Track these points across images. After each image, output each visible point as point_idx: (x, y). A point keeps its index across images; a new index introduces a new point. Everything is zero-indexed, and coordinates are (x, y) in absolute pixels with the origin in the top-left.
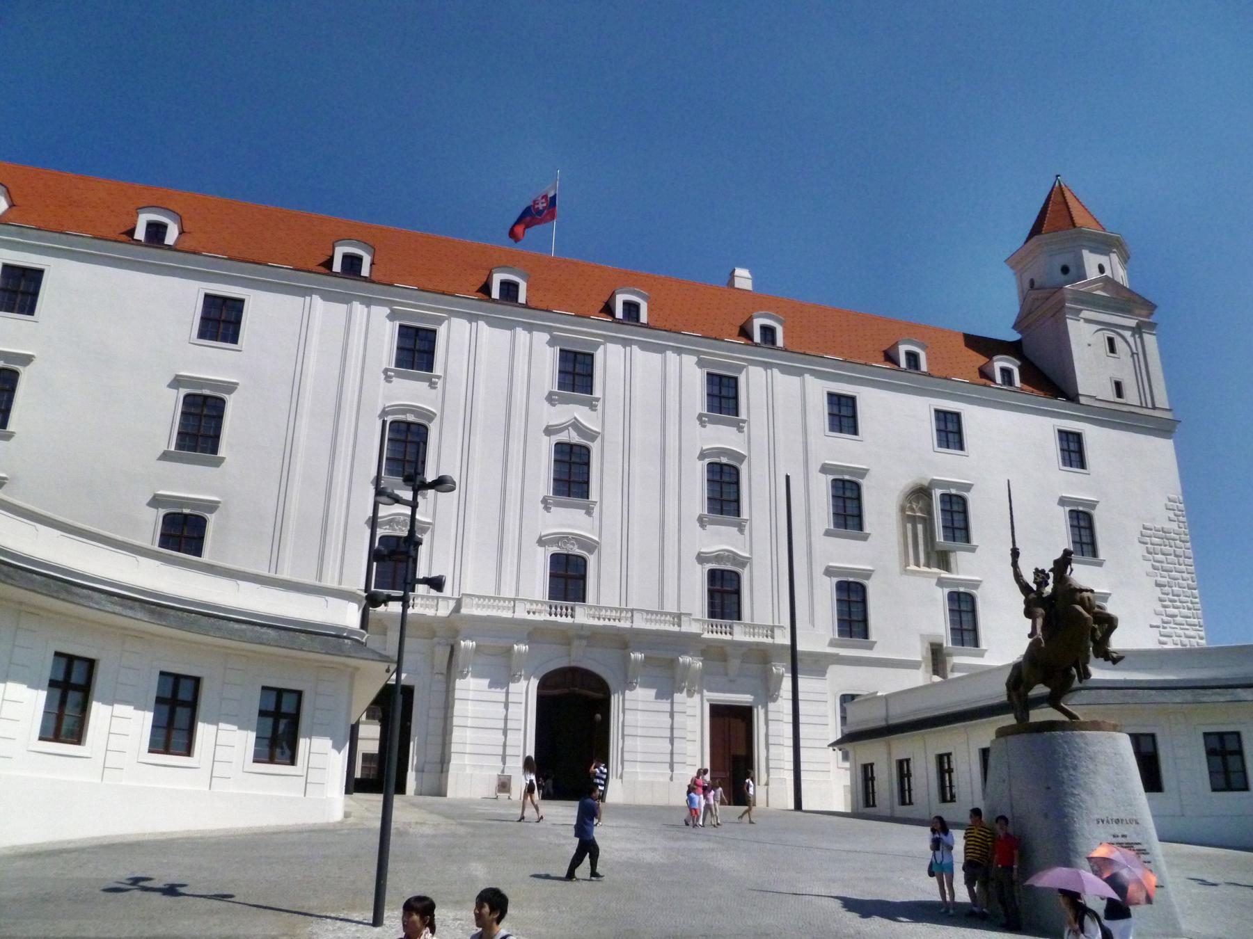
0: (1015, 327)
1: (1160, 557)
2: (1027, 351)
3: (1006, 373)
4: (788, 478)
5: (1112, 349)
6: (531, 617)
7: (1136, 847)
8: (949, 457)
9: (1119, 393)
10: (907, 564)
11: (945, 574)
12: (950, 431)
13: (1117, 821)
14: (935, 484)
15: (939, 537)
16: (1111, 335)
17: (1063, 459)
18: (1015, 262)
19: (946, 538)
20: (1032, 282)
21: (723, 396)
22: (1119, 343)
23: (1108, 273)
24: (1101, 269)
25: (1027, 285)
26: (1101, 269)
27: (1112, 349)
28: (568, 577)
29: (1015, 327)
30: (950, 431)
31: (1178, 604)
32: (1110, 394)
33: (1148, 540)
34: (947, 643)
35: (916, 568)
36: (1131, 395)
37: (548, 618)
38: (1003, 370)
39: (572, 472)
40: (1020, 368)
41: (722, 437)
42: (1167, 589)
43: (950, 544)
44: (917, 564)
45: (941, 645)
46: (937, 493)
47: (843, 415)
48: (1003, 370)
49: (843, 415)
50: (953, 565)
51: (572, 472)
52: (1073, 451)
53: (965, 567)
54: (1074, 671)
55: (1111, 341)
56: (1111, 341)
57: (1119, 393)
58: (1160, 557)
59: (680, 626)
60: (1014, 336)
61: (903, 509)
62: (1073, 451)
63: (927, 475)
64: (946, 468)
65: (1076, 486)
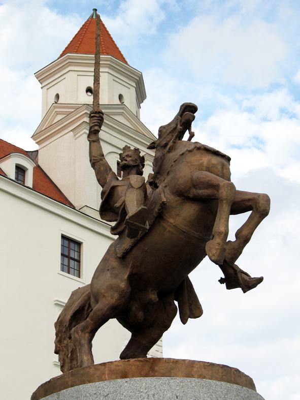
0: (33, 137)
3: (20, 170)
17: (62, 264)
18: (45, 76)
20: (57, 96)
23: (126, 101)
24: (121, 97)
25: (52, 99)
26: (121, 97)
29: (33, 137)
40: (34, 168)
54: (176, 303)
60: (31, 146)
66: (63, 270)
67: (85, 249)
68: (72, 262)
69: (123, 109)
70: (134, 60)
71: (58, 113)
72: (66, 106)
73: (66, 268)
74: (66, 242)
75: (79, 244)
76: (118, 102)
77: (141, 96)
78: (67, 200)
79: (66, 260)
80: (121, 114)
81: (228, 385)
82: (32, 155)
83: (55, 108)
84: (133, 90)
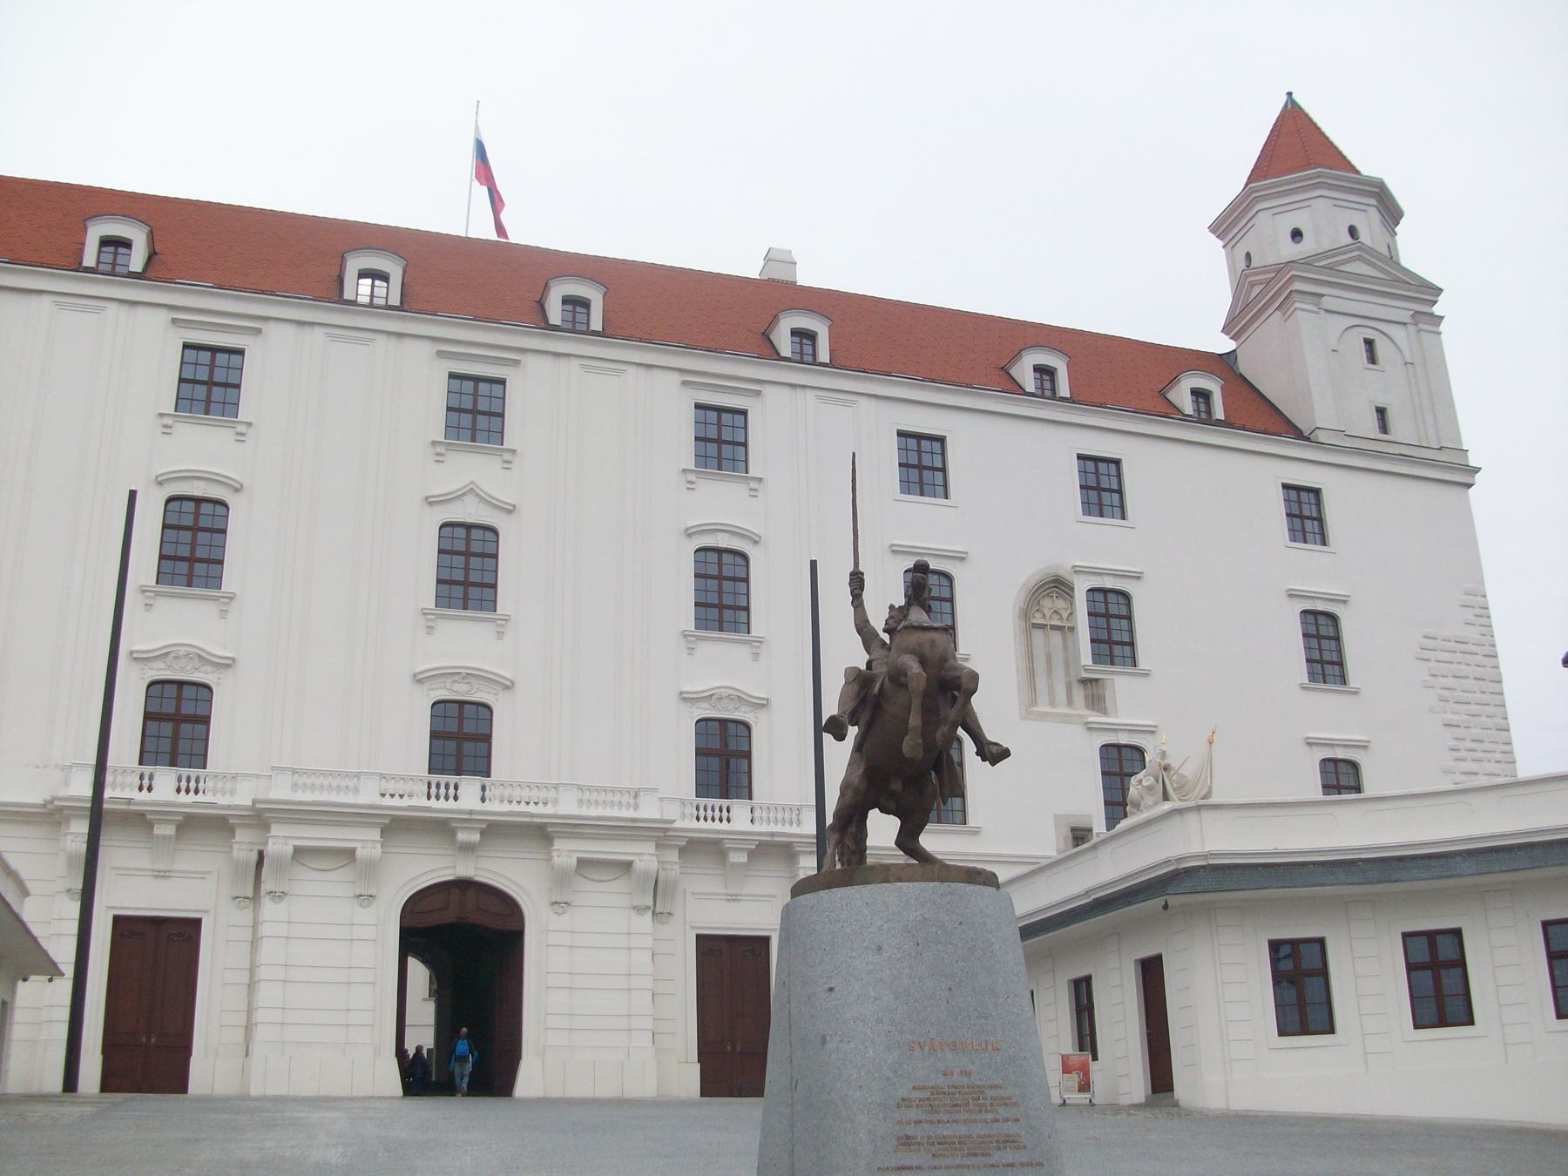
0: (1225, 330)
1: (1450, 682)
2: (1244, 367)
4: (813, 564)
5: (1372, 359)
6: (387, 801)
7: (990, 1093)
8: (1104, 530)
9: (1384, 428)
10: (1034, 702)
11: (1095, 718)
12: (1102, 487)
13: (954, 1047)
14: (1078, 571)
15: (1086, 656)
16: (1371, 334)
17: (1291, 530)
18: (1227, 226)
19: (1097, 658)
20: (1248, 256)
21: (721, 441)
22: (1381, 347)
23: (1364, 237)
24: (1352, 231)
25: (1242, 264)
26: (1352, 231)
27: (1372, 359)
28: (461, 738)
29: (1225, 330)
30: (1102, 487)
31: (1480, 755)
32: (1369, 426)
33: (1430, 655)
34: (1099, 826)
35: (1049, 709)
36: (1401, 428)
37: (424, 802)
38: (1196, 393)
39: (467, 568)
40: (1222, 388)
41: (721, 505)
42: (1460, 732)
43: (1101, 671)
44: (1052, 704)
45: (1090, 830)
46: (1081, 586)
47: (923, 464)
48: (1196, 393)
49: (923, 464)
50: (1109, 704)
51: (467, 568)
52: (1305, 514)
53: (1132, 704)
55: (1369, 343)
56: (1369, 343)
57: (1384, 428)
58: (1450, 682)
59: (636, 807)
60: (1224, 345)
61: (1025, 614)
62: (1305, 514)
63: (1063, 560)
64: (1095, 549)
65: (1312, 573)
66: (1293, 539)
67: (1326, 497)
68: (1308, 523)
69: (1358, 249)
70: (1367, 165)
71: (1252, 285)
72: (1264, 269)
73: (1299, 535)
74: (1293, 494)
75: (1317, 492)
76: (1349, 240)
77: (1391, 213)
78: (1288, 422)
79: (1297, 521)
80: (1359, 258)
81: (923, 884)
82: (1222, 364)
83: (1247, 276)
84: (1374, 213)
